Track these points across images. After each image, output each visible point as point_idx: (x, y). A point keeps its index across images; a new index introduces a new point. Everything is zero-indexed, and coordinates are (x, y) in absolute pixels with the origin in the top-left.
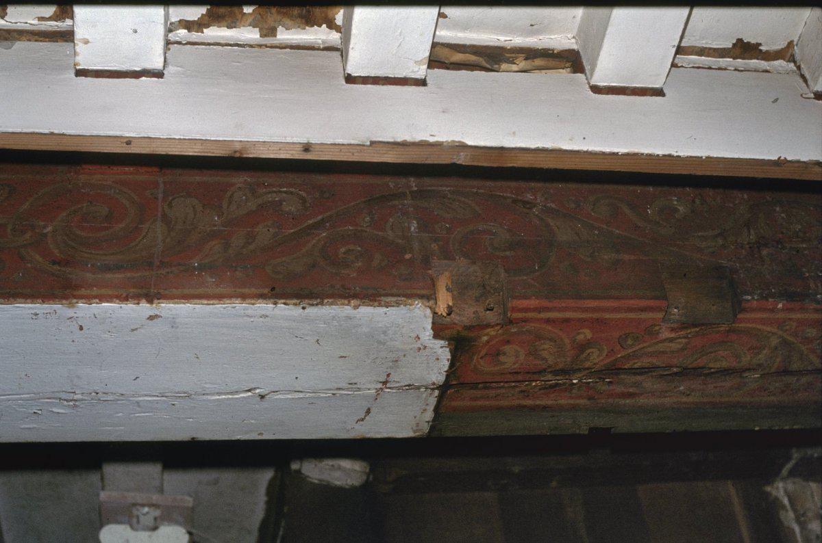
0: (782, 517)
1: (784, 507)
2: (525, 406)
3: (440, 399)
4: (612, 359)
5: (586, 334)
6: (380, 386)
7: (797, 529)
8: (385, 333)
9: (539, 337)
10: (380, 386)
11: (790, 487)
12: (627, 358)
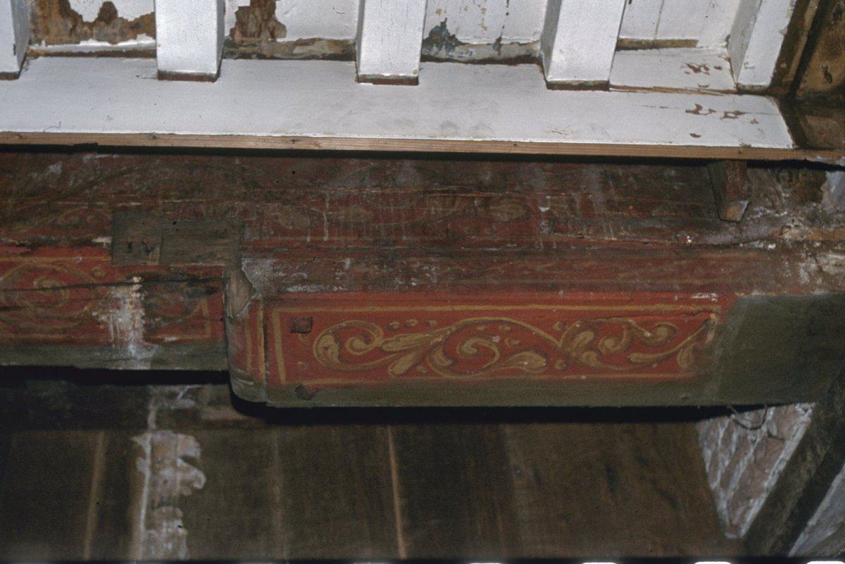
0: (137, 463)
1: (144, 456)
7: (148, 474)
11: (158, 437)
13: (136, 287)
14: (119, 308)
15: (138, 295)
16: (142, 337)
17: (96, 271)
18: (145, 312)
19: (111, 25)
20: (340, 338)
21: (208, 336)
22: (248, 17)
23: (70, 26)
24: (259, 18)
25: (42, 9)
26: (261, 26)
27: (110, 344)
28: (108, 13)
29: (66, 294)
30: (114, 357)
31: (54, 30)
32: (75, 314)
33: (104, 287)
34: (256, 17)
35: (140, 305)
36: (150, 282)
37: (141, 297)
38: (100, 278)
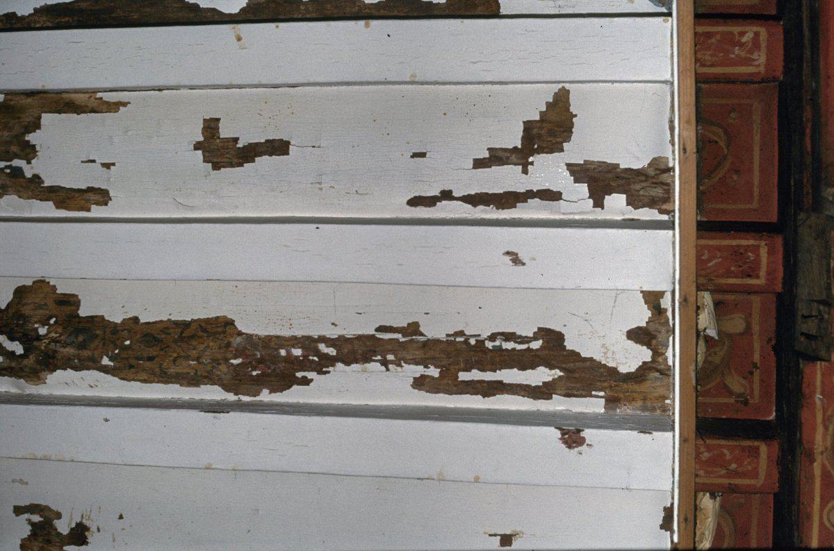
19: (657, 333)
22: (643, 196)
23: (657, 374)
24: (644, 184)
25: (634, 400)
26: (653, 183)
28: (638, 335)
31: (661, 391)
34: (643, 188)
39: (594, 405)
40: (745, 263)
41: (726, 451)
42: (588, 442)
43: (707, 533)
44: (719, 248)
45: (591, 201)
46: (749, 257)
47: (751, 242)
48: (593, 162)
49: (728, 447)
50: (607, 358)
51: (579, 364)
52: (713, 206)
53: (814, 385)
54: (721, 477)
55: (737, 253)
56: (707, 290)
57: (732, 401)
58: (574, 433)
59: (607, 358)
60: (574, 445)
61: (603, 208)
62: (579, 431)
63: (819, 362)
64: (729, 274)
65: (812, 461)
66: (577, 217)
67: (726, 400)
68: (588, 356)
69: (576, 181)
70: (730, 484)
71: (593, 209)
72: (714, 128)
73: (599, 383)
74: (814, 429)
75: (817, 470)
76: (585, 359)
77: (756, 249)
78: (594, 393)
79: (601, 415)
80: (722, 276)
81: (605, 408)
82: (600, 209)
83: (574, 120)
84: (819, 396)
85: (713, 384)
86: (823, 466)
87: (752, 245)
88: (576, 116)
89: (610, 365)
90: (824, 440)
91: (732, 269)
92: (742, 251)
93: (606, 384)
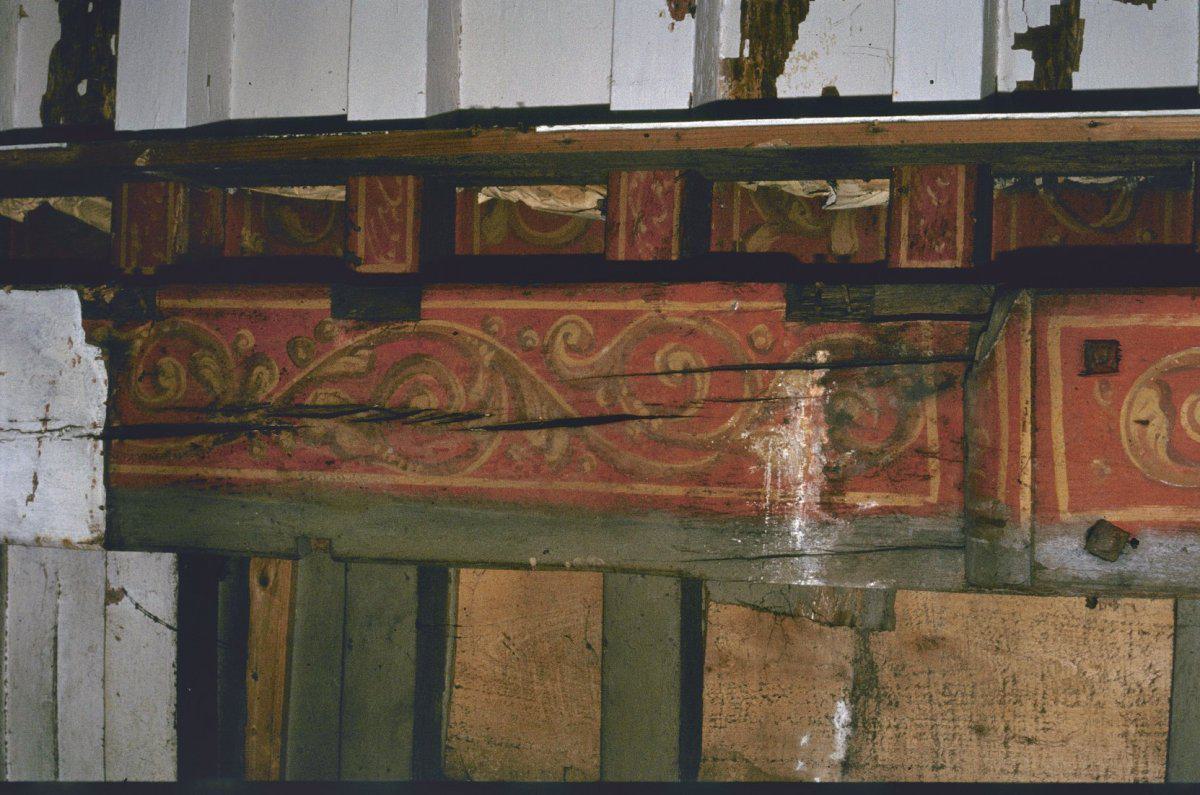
2: (200, 481)
3: (106, 453)
4: (287, 387)
5: (248, 339)
6: (39, 426)
8: (38, 332)
9: (197, 344)
10: (39, 426)
12: (309, 383)
13: (819, 374)
14: (786, 421)
15: (821, 391)
16: (818, 499)
17: (758, 334)
18: (830, 433)
20: (1169, 406)
21: (933, 498)
27: (761, 513)
29: (703, 385)
30: (764, 552)
32: (710, 435)
33: (767, 371)
35: (822, 416)
36: (840, 369)
37: (825, 396)
38: (758, 351)
39: (730, 43)
40: (931, 240)
41: (664, 216)
42: (678, 24)
43: (552, 201)
44: (952, 202)
45: (1024, 30)
46: (938, 244)
47: (960, 247)
48: (1082, 34)
49: (670, 220)
50: (798, 60)
51: (788, 22)
52: (1014, 208)
53: (754, 300)
54: (629, 211)
55: (945, 226)
56: (891, 192)
57: (736, 237)
58: (690, 4)
59: (798, 60)
60: (673, 6)
61: (1014, 48)
62: (693, 11)
63: (785, 304)
64: (915, 216)
65: (648, 298)
66: (1001, 12)
67: (736, 228)
68: (801, 32)
69: (1054, 9)
70: (619, 224)
71: (1012, 34)
72: (1128, 208)
73: (761, 48)
74: (691, 300)
75: (633, 305)
76: (795, 29)
77: (952, 255)
78: (747, 41)
79: (716, 53)
80: (912, 205)
81: (727, 59)
82: (1013, 44)
83: (1144, 6)
84: (737, 305)
85: (759, 210)
86: (641, 313)
87: (956, 249)
88: (1150, 8)
89: (788, 65)
90: (679, 314)
91: (922, 221)
92: (949, 234)
93: (759, 58)
